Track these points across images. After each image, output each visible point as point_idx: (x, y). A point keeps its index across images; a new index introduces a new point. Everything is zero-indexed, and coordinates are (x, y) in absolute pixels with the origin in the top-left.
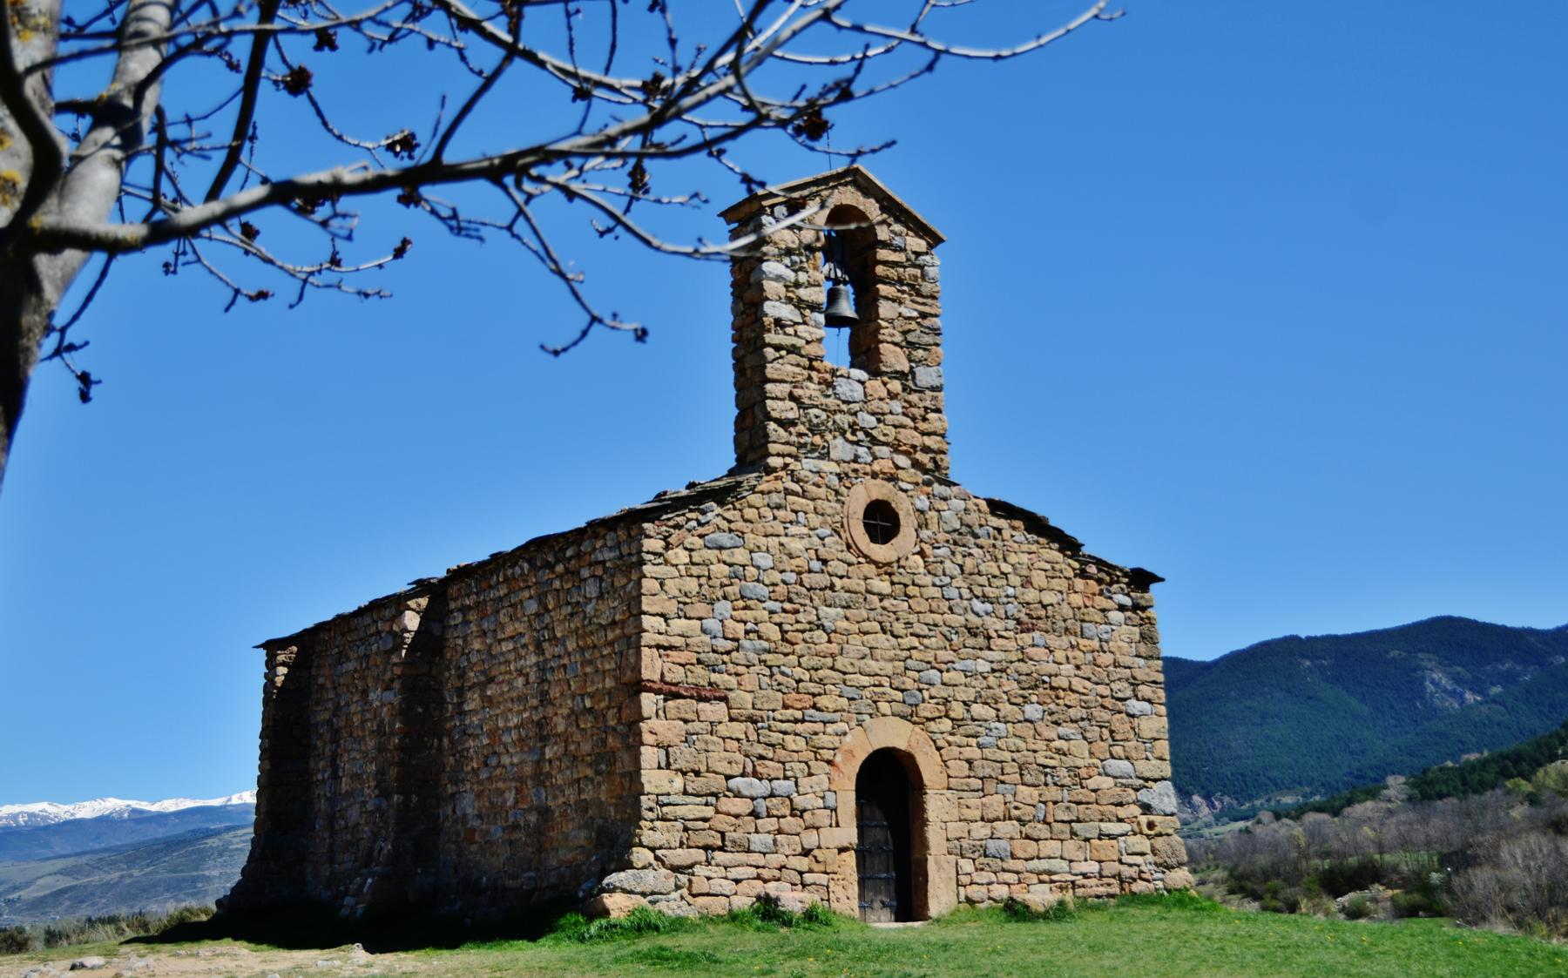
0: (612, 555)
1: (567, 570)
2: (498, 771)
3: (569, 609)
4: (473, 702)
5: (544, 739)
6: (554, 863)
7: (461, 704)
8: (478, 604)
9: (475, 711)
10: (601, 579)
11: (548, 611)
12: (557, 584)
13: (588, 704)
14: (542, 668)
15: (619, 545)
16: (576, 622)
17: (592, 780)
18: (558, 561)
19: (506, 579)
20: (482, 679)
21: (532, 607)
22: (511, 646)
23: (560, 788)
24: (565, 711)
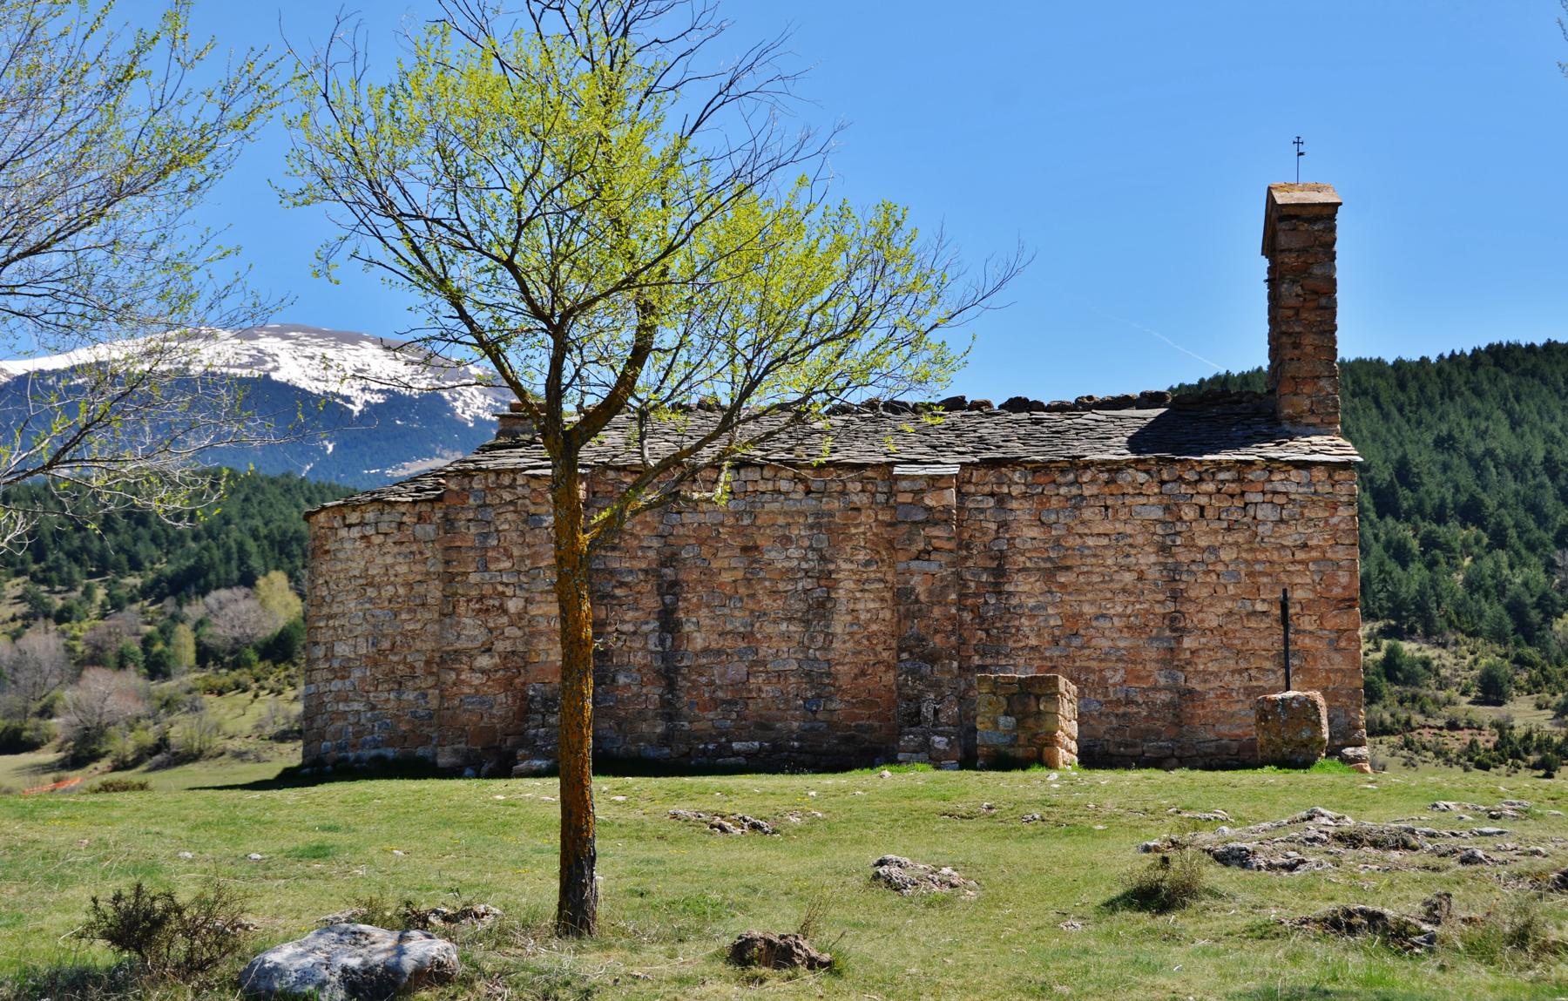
0: (1301, 490)
1: (1219, 491)
2: (1087, 652)
3: (1225, 525)
4: (1025, 588)
5: (1183, 631)
6: (1212, 736)
7: (997, 584)
8: (1024, 496)
9: (1030, 595)
10: (1282, 507)
11: (1180, 519)
12: (1203, 500)
13: (1260, 607)
14: (1172, 574)
15: (1310, 484)
16: (1240, 537)
17: (1274, 672)
18: (1201, 480)
19: (1093, 481)
20: (1049, 565)
21: (1158, 513)
22: (1105, 541)
23: (1216, 675)
24: (1221, 611)
